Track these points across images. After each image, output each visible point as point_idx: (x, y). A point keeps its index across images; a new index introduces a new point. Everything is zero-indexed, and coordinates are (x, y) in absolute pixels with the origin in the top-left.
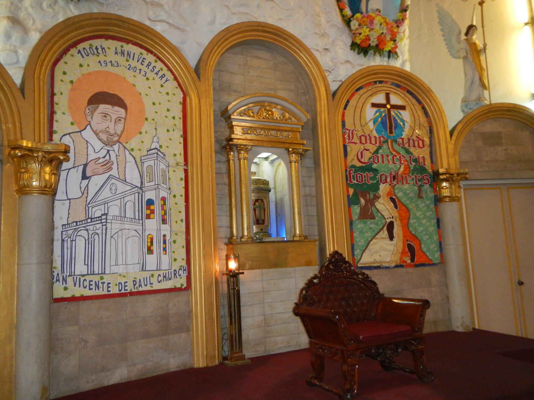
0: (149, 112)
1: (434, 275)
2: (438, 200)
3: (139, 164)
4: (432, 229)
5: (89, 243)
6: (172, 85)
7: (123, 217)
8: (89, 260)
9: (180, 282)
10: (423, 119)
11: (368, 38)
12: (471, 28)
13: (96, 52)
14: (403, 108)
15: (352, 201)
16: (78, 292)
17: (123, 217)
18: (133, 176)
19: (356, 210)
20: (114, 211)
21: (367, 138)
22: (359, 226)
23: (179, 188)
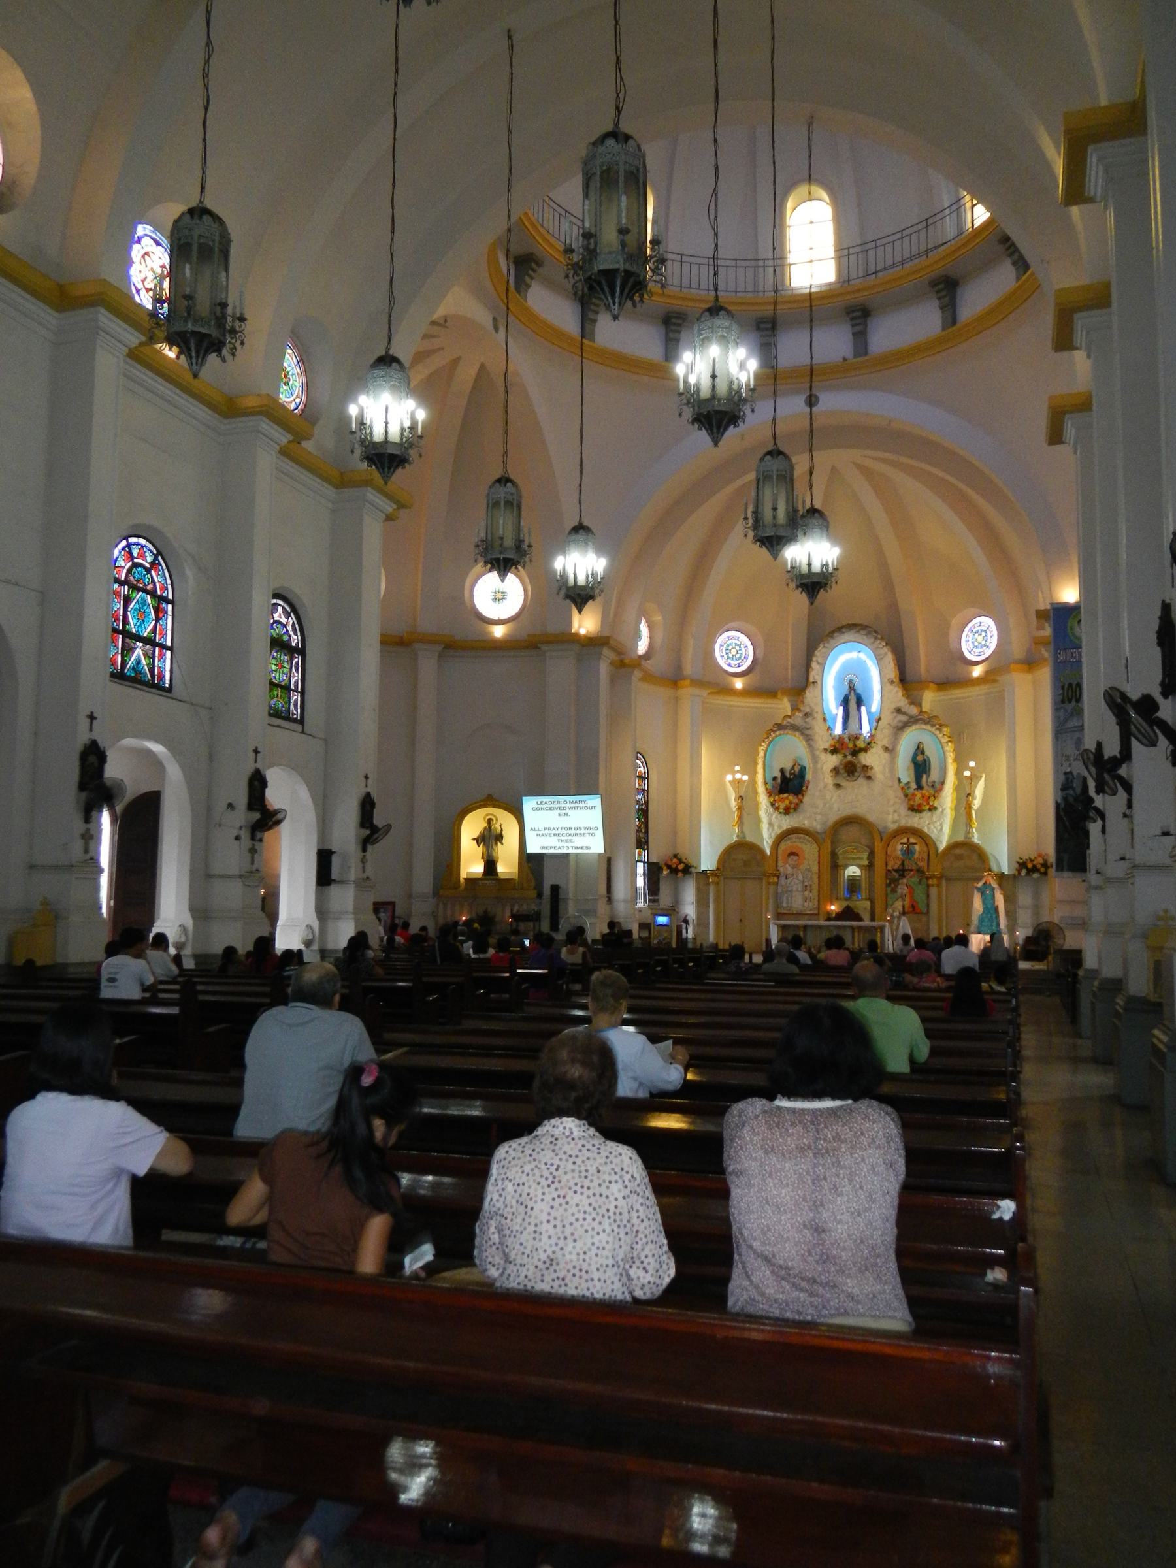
0: (806, 856)
1: (924, 919)
2: (928, 886)
3: (803, 874)
4: (924, 898)
5: (787, 898)
6: (815, 846)
7: (797, 890)
8: (787, 903)
9: (816, 912)
10: (925, 849)
11: (913, 806)
12: (969, 794)
13: (789, 839)
14: (915, 844)
15: (888, 885)
16: (783, 911)
17: (797, 890)
18: (801, 878)
19: (889, 889)
20: (794, 889)
21: (897, 858)
22: (890, 896)
23: (816, 880)
